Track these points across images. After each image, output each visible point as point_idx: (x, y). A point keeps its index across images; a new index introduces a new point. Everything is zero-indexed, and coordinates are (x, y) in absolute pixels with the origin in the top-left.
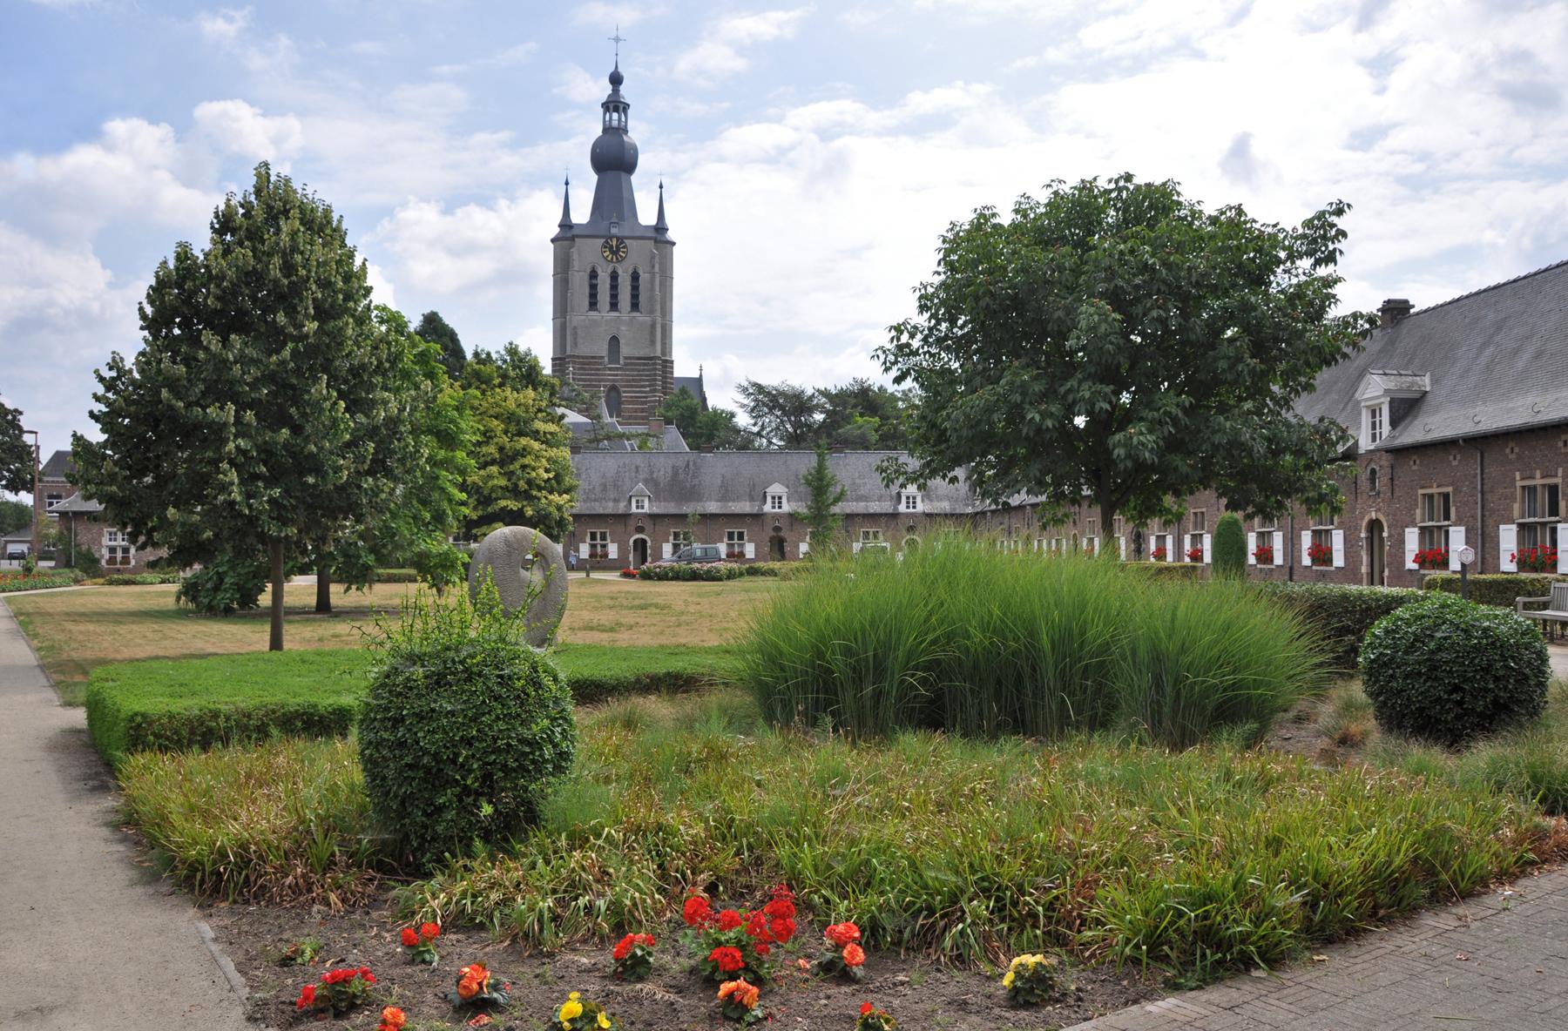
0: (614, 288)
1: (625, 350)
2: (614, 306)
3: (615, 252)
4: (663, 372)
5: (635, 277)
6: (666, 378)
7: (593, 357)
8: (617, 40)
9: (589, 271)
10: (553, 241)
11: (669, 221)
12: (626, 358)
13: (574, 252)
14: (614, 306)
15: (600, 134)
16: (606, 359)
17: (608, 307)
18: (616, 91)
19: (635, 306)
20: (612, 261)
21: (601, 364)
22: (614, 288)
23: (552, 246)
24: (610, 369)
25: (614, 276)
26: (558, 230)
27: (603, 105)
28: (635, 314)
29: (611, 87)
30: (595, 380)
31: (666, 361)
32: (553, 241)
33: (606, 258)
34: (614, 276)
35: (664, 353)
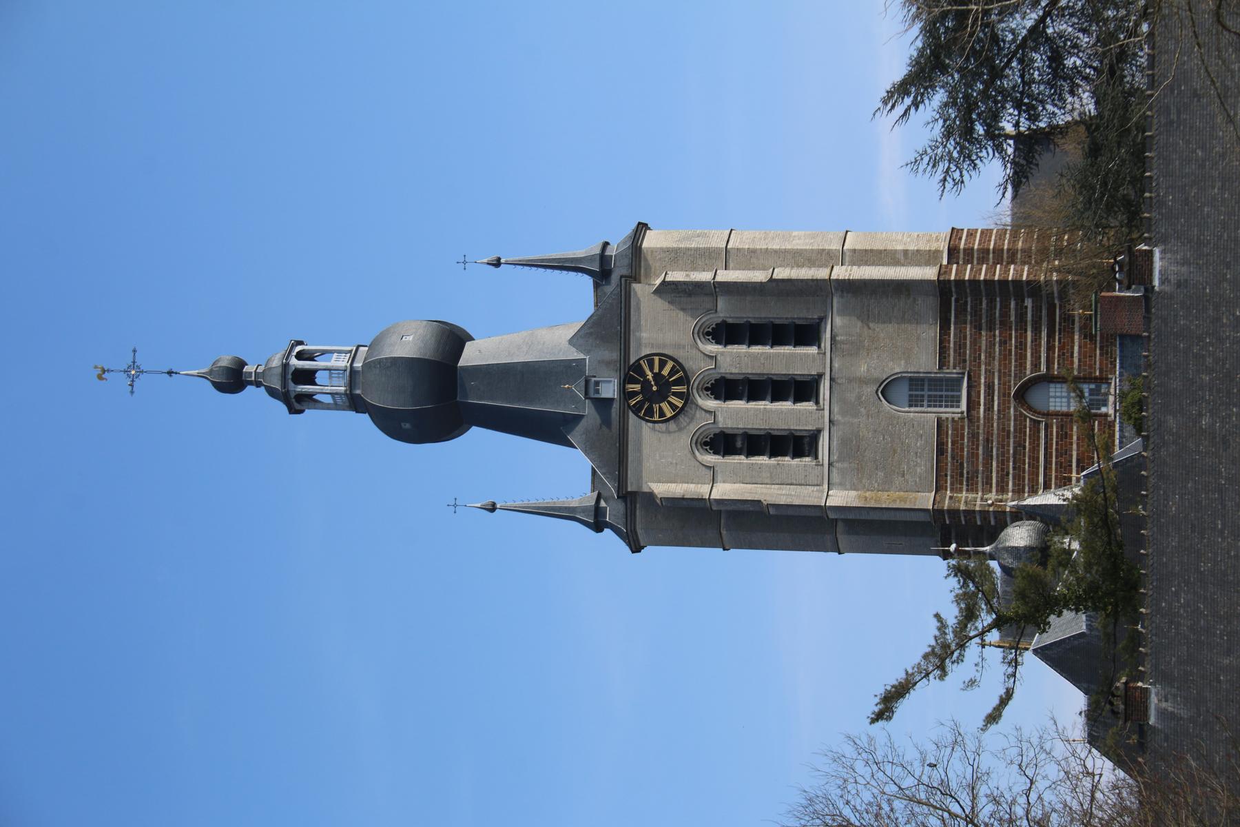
0: (755, 388)
1: (924, 361)
2: (804, 389)
3: (664, 387)
4: (982, 260)
5: (726, 333)
6: (998, 252)
7: (941, 450)
8: (134, 372)
9: (710, 459)
10: (636, 548)
11: (586, 248)
12: (943, 363)
13: (662, 489)
14: (804, 389)
15: (367, 415)
16: (948, 413)
17: (808, 406)
18: (251, 383)
19: (806, 334)
20: (686, 397)
21: (958, 436)
22: (755, 388)
23: (649, 551)
24: (973, 405)
25: (726, 388)
26: (605, 529)
27: (293, 411)
28: (827, 335)
29: (250, 389)
30: (1003, 446)
31: (953, 252)
32: (636, 548)
33: (679, 412)
34: (726, 388)
35: (929, 257)
